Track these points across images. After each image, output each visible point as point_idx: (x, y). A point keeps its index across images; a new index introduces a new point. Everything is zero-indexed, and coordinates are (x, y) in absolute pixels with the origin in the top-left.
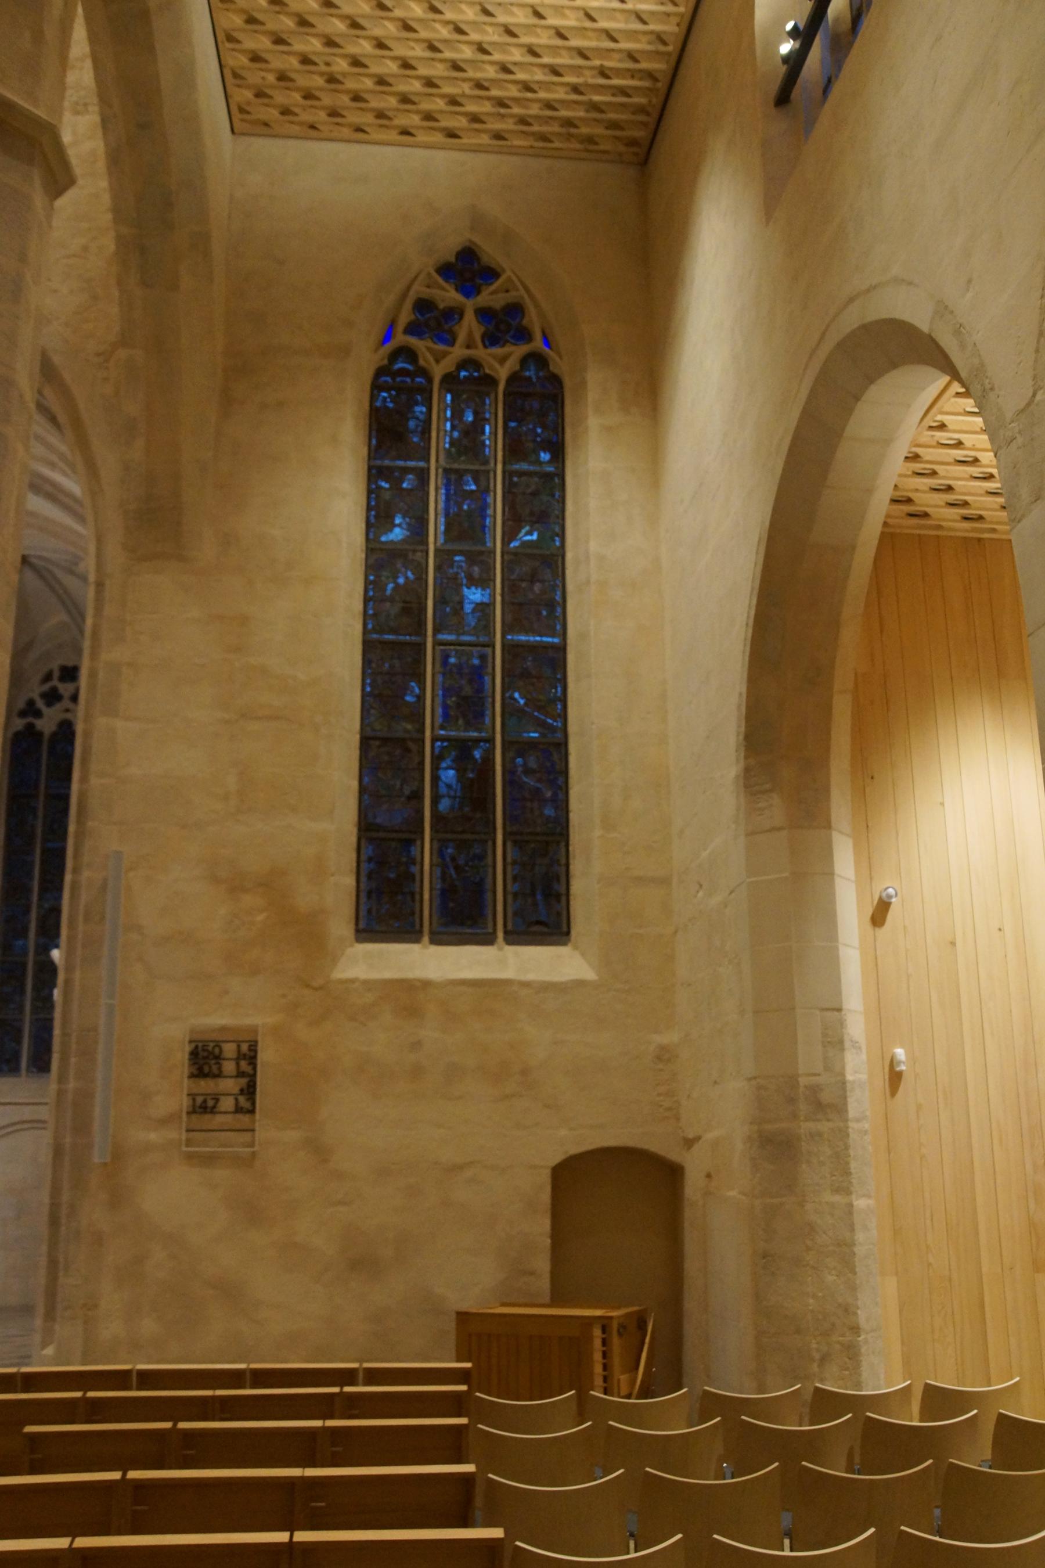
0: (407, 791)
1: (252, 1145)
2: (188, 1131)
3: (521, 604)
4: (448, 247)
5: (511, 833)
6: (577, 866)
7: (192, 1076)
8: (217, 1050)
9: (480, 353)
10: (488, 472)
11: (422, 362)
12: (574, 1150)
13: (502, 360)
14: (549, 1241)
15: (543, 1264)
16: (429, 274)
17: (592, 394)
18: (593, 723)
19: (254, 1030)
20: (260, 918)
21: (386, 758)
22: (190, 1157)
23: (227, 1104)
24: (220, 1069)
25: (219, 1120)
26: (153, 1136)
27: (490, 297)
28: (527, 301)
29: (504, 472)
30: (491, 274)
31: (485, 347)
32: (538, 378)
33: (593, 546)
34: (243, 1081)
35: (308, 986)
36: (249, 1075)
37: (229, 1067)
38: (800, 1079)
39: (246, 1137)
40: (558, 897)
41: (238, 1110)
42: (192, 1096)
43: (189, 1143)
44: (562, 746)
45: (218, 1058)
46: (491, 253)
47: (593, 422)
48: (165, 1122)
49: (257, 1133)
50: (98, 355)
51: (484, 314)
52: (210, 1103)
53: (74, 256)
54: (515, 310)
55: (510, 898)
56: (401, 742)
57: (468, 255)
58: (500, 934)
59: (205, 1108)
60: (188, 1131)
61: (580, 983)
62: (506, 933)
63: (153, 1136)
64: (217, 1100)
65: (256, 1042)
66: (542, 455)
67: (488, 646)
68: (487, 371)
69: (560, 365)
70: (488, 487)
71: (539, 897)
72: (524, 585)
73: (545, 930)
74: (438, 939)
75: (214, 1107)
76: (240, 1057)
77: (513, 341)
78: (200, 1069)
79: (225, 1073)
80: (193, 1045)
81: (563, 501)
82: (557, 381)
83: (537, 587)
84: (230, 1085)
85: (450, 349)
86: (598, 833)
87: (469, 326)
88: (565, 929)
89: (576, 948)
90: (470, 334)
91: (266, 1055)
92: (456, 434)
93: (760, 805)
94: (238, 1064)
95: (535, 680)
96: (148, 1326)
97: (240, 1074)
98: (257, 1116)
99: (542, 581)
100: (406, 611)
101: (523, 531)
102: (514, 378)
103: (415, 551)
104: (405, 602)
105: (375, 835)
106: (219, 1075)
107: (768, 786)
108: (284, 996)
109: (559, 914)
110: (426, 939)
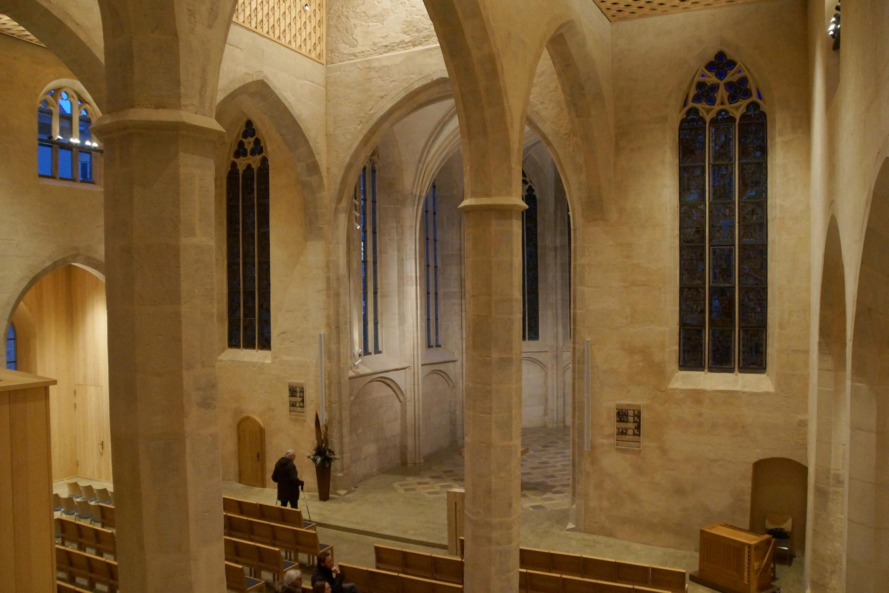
0: (699, 310)
1: (639, 447)
2: (617, 440)
3: (747, 226)
4: (710, 56)
5: (742, 327)
6: (770, 341)
7: (617, 421)
8: (626, 412)
9: (727, 106)
10: (732, 164)
11: (701, 114)
12: (762, 458)
13: (738, 108)
14: (751, 490)
15: (748, 498)
16: (702, 70)
17: (778, 125)
18: (776, 283)
19: (639, 406)
20: (641, 364)
21: (690, 296)
22: (617, 449)
23: (630, 432)
24: (627, 419)
25: (627, 438)
26: (605, 441)
28: (749, 77)
29: (739, 164)
30: (732, 64)
31: (730, 103)
32: (755, 115)
33: (778, 201)
35: (659, 390)
36: (638, 422)
37: (631, 419)
38: (831, 471)
40: (762, 353)
41: (634, 434)
42: (618, 429)
43: (617, 445)
44: (765, 290)
45: (627, 415)
46: (731, 54)
47: (779, 140)
48: (609, 436)
51: (729, 86)
52: (625, 431)
53: (552, 91)
54: (744, 81)
55: (741, 353)
56: (697, 289)
57: (720, 55)
58: (736, 369)
59: (623, 433)
60: (617, 440)
61: (768, 393)
62: (739, 368)
63: (605, 441)
64: (627, 430)
65: (640, 410)
66: (757, 153)
67: (733, 246)
68: (731, 114)
69: (764, 107)
70: (732, 172)
71: (754, 353)
72: (748, 217)
73: (756, 367)
74: (711, 370)
75: (626, 433)
76: (634, 415)
77: (743, 97)
78: (621, 419)
79: (629, 421)
80: (618, 410)
81: (766, 175)
82: (763, 115)
83: (755, 217)
84: (631, 425)
85: (713, 107)
86: (777, 330)
87: (722, 94)
88: (764, 367)
89: (768, 375)
90: (722, 97)
91: (644, 415)
92: (717, 148)
93: (824, 359)
94: (634, 418)
95: (753, 260)
96: (605, 503)
97: (635, 422)
99: (757, 214)
100: (697, 232)
101: (748, 191)
102: (743, 117)
103: (700, 205)
104: (697, 228)
105: (686, 327)
106: (627, 422)
107: (828, 352)
108: (650, 394)
109: (762, 361)
110: (706, 370)
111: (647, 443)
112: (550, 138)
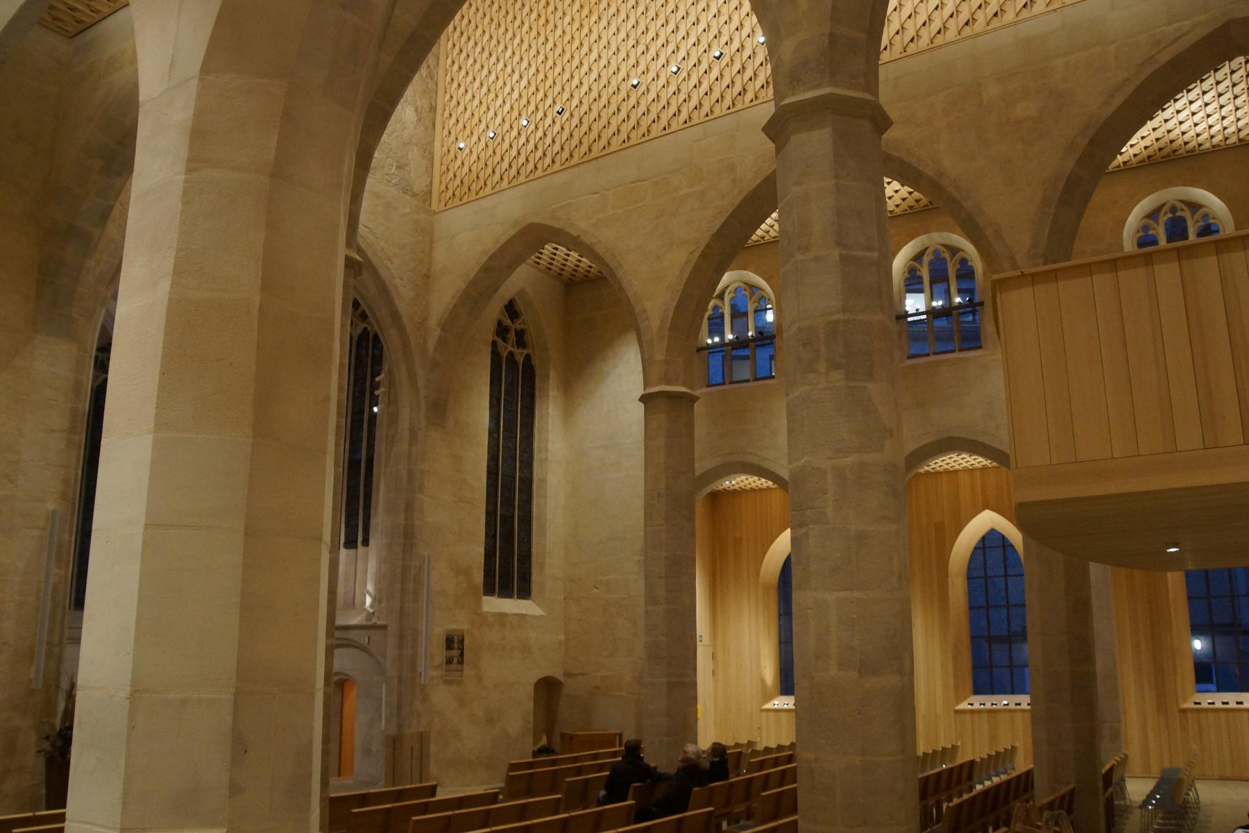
1: (462, 676)
2: (446, 671)
19: (463, 631)
20: (464, 585)
22: (445, 681)
23: (455, 661)
26: (434, 673)
27: (508, 322)
34: (460, 651)
37: (456, 645)
39: (459, 673)
49: (464, 672)
50: (419, 323)
58: (516, 595)
60: (446, 671)
63: (434, 673)
74: (500, 596)
84: (455, 653)
89: (534, 602)
97: (459, 649)
98: (464, 665)
106: (453, 649)
110: (497, 596)
111: (468, 672)
112: (405, 320)
